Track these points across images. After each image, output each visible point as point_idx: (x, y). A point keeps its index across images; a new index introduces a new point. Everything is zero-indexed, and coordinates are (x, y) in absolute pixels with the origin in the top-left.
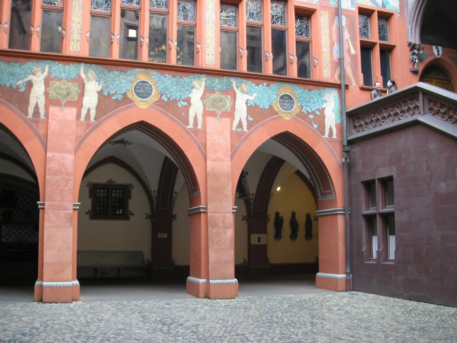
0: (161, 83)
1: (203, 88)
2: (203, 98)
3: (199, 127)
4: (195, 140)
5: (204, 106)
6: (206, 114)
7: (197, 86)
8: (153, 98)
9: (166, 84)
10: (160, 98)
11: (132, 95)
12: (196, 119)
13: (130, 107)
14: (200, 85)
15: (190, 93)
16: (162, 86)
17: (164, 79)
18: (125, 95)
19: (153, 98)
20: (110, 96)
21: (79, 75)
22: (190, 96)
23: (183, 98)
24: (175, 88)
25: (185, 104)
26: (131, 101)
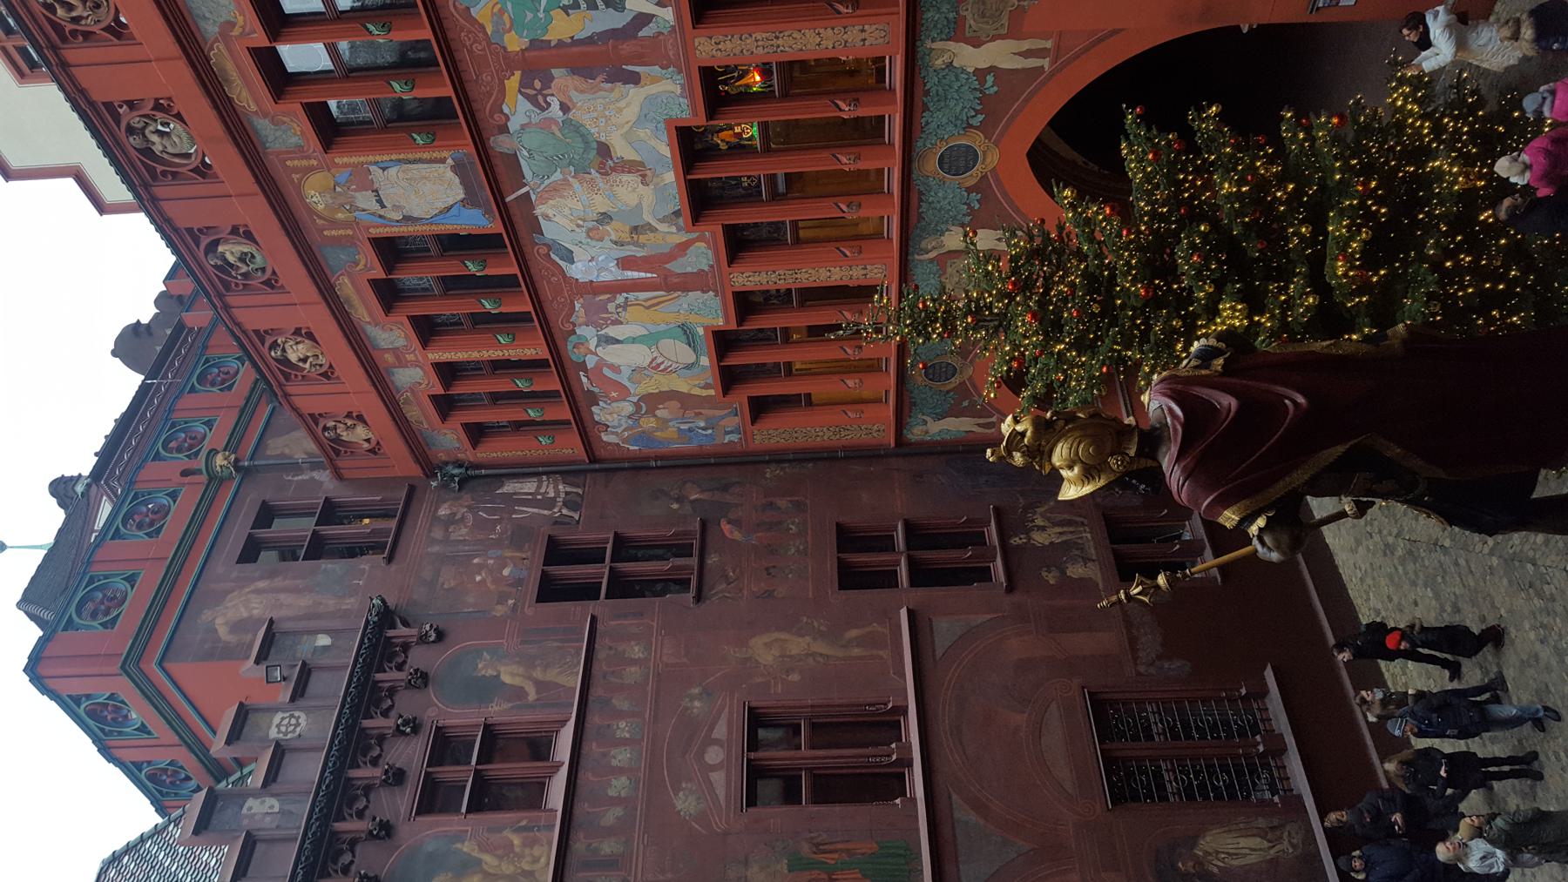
0: (944, 129)
1: (951, 45)
2: (977, 43)
3: (1049, 44)
4: (1077, 56)
5: (994, 39)
6: (1014, 33)
7: (946, 58)
8: (977, 141)
9: (944, 120)
10: (976, 128)
11: (972, 178)
12: (1027, 54)
13: (999, 184)
14: (943, 51)
15: (963, 71)
16: (950, 128)
17: (933, 125)
18: (969, 190)
19: (977, 141)
20: (972, 212)
21: (931, 261)
22: (971, 70)
23: (976, 85)
24: (952, 104)
25: (990, 79)
26: (984, 177)
